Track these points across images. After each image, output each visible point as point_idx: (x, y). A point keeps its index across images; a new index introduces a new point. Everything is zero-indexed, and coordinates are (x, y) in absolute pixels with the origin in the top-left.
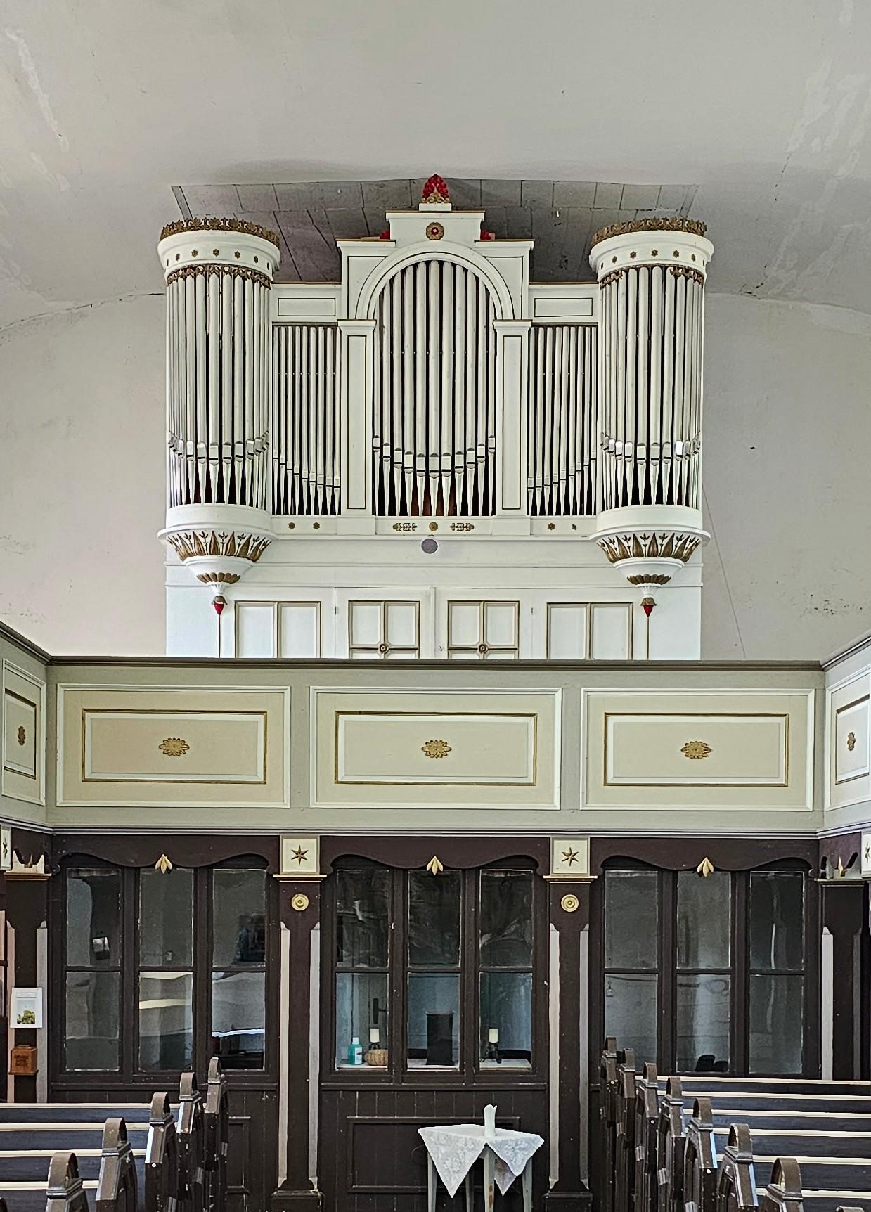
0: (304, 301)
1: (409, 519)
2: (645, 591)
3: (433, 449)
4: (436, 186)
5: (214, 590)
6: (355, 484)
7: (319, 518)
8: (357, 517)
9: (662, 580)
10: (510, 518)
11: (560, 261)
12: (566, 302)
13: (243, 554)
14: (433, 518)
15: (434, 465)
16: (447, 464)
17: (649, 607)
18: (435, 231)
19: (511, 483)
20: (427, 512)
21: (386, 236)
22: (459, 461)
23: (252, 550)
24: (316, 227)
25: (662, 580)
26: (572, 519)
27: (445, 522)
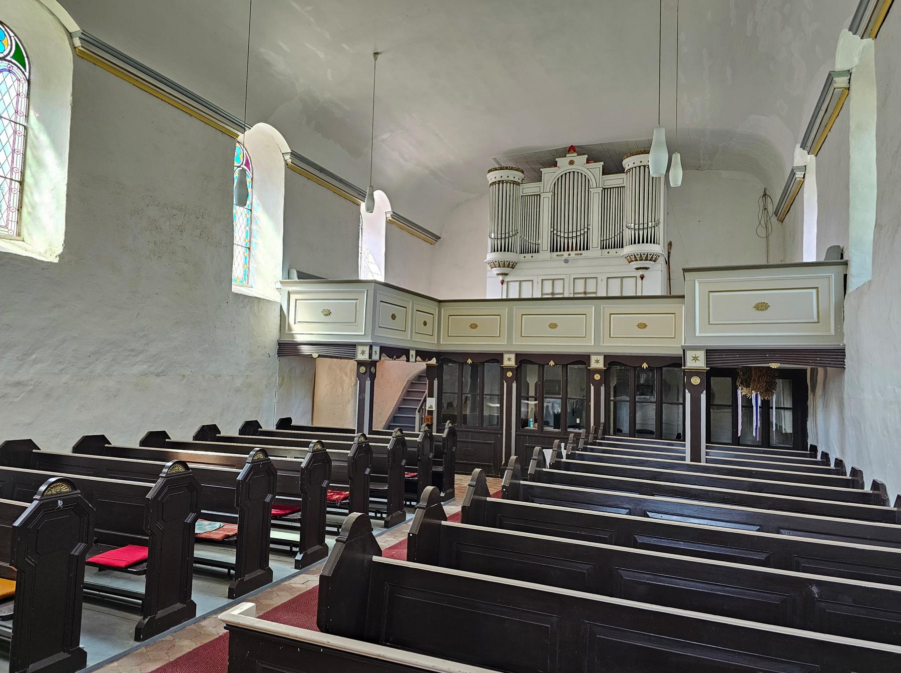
0: (530, 188)
1: (562, 253)
2: (641, 272)
3: (570, 230)
4: (572, 149)
5: (501, 278)
6: (545, 242)
7: (534, 254)
8: (545, 253)
9: (647, 268)
10: (595, 251)
11: (613, 167)
12: (613, 180)
13: (508, 267)
14: (570, 252)
15: (570, 235)
16: (574, 235)
17: (642, 277)
18: (572, 163)
19: (595, 239)
20: (568, 250)
21: (556, 166)
22: (579, 234)
23: (512, 266)
24: (535, 164)
25: (647, 268)
26: (616, 250)
27: (573, 253)
